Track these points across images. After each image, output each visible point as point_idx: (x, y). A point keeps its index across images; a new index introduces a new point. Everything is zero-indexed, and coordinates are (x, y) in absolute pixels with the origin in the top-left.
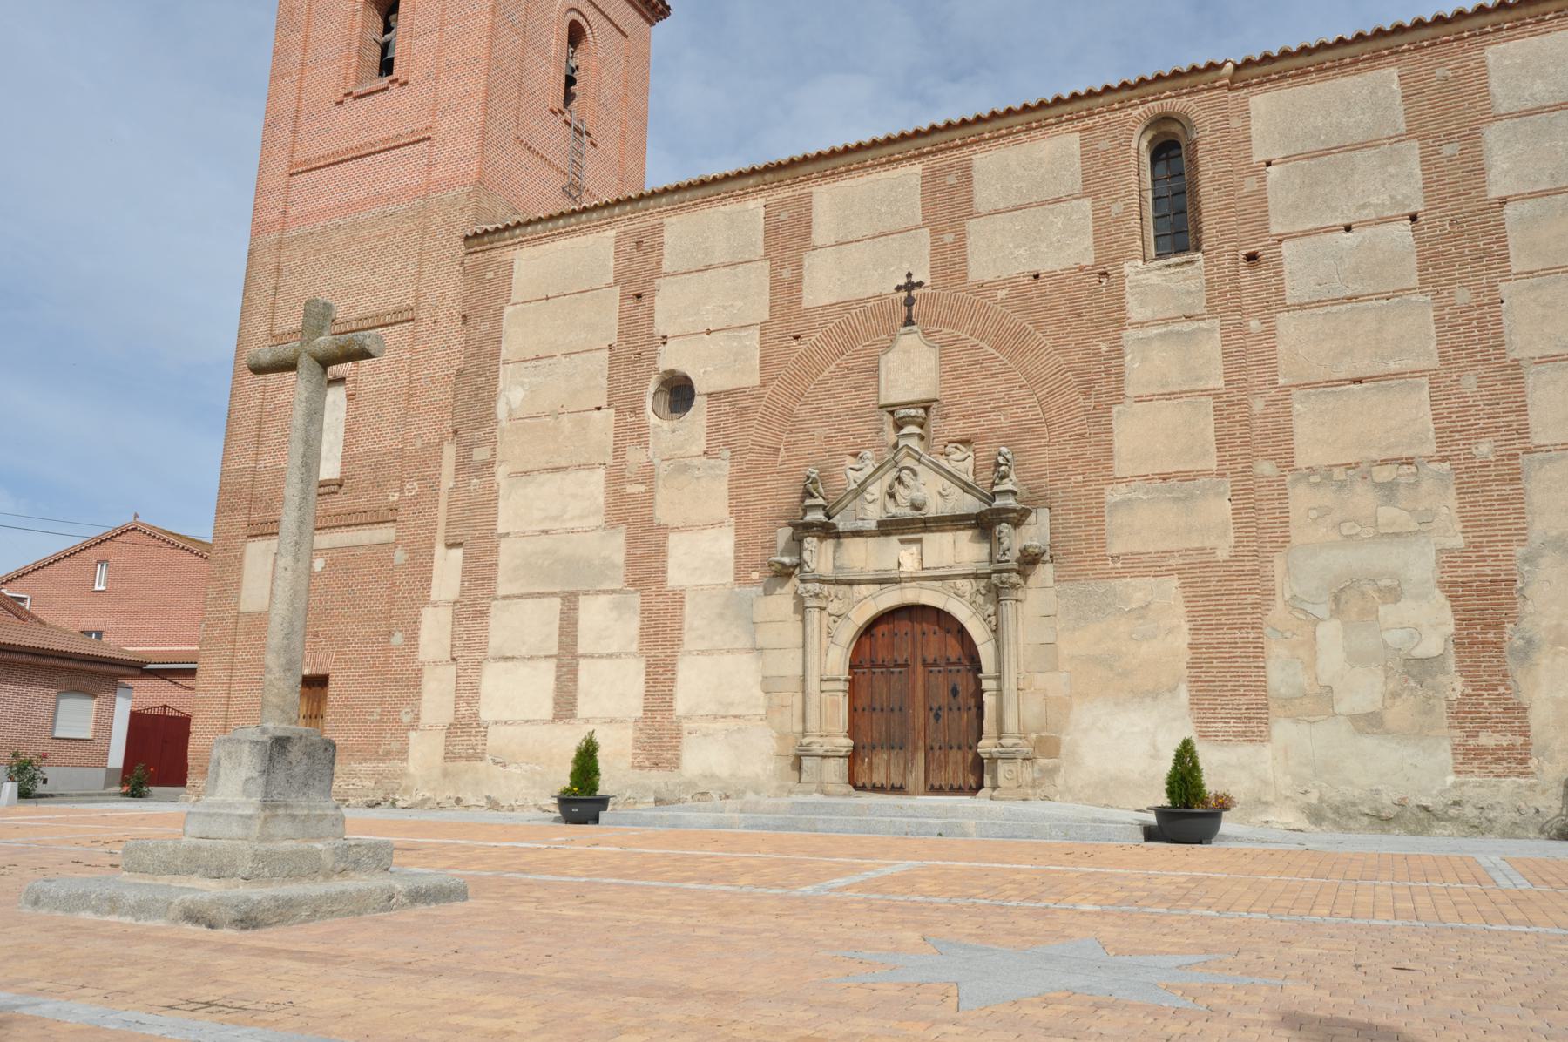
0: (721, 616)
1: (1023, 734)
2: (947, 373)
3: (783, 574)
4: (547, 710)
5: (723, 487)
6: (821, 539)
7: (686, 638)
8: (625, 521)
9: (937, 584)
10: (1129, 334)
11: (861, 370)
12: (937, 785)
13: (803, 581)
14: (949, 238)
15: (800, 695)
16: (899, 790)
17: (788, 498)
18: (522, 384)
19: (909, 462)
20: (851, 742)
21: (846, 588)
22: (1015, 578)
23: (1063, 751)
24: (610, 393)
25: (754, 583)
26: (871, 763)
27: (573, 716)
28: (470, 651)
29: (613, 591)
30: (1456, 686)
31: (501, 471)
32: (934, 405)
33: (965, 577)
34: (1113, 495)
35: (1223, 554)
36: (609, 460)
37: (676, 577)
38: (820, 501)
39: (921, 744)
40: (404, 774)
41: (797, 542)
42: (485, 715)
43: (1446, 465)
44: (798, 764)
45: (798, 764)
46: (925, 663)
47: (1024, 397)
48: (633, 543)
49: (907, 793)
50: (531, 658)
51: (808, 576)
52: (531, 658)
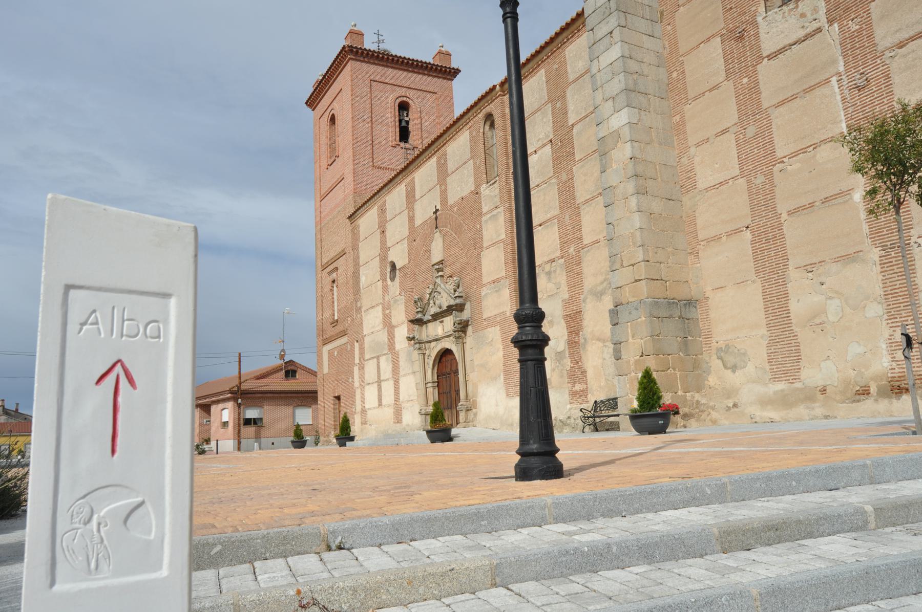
2: (446, 248)
4: (377, 405)
10: (484, 218)
14: (443, 187)
30: (568, 363)
31: (363, 310)
43: (563, 260)
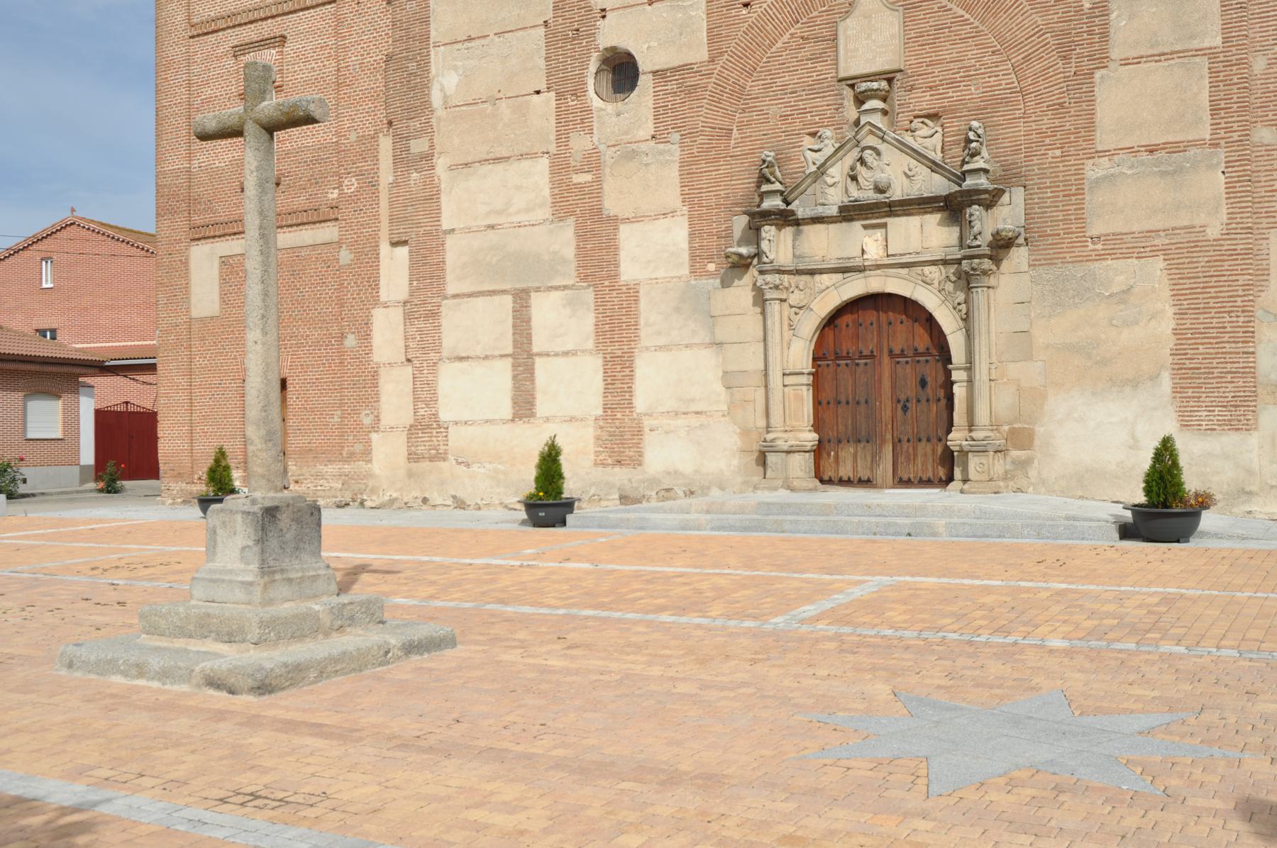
0: (677, 310)
1: (995, 426)
3: (740, 265)
4: (506, 410)
5: (674, 174)
6: (780, 227)
7: (642, 333)
8: (572, 213)
9: (904, 271)
11: (817, 39)
12: (905, 478)
13: (762, 272)
15: (762, 390)
16: (866, 483)
17: (744, 183)
18: (455, 68)
19: (871, 141)
20: (816, 436)
21: (807, 278)
22: (987, 264)
23: (1037, 442)
24: (549, 75)
25: (710, 275)
26: (837, 457)
27: (532, 415)
28: (424, 352)
29: (565, 287)
31: (441, 163)
32: (899, 76)
33: (933, 263)
34: (1095, 170)
35: (1213, 232)
36: (553, 148)
37: (629, 271)
38: (778, 186)
39: (889, 436)
40: (370, 475)
41: (754, 231)
42: (444, 416)
44: (762, 460)
45: (762, 460)
46: (891, 353)
47: (997, 64)
48: (582, 236)
49: (875, 487)
50: (486, 357)
51: (767, 267)
52: (486, 357)
